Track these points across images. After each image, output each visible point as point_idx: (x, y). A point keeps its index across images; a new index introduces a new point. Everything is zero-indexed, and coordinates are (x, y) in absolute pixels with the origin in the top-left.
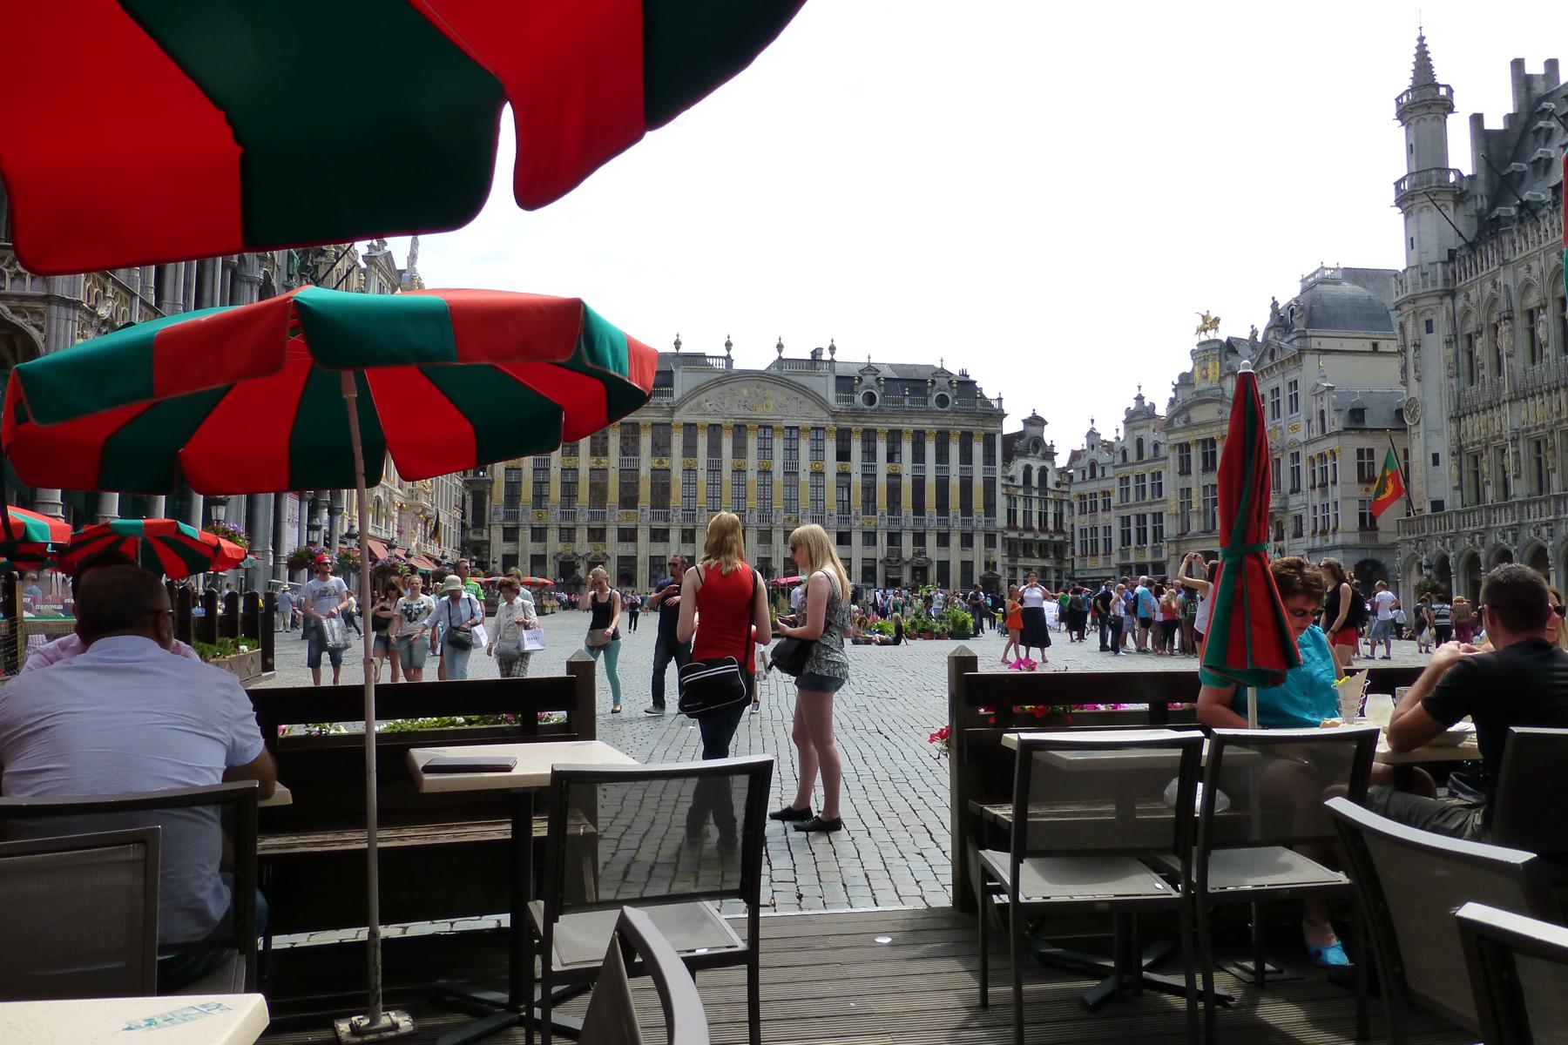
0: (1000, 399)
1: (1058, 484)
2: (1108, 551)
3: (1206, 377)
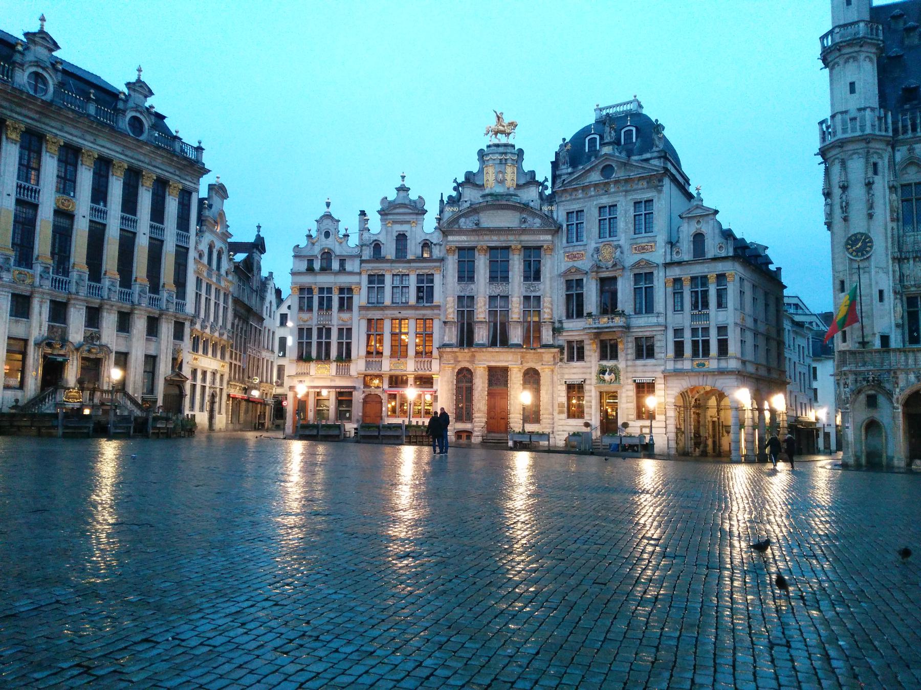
0: (199, 149)
1: (227, 273)
2: (345, 357)
3: (502, 182)
